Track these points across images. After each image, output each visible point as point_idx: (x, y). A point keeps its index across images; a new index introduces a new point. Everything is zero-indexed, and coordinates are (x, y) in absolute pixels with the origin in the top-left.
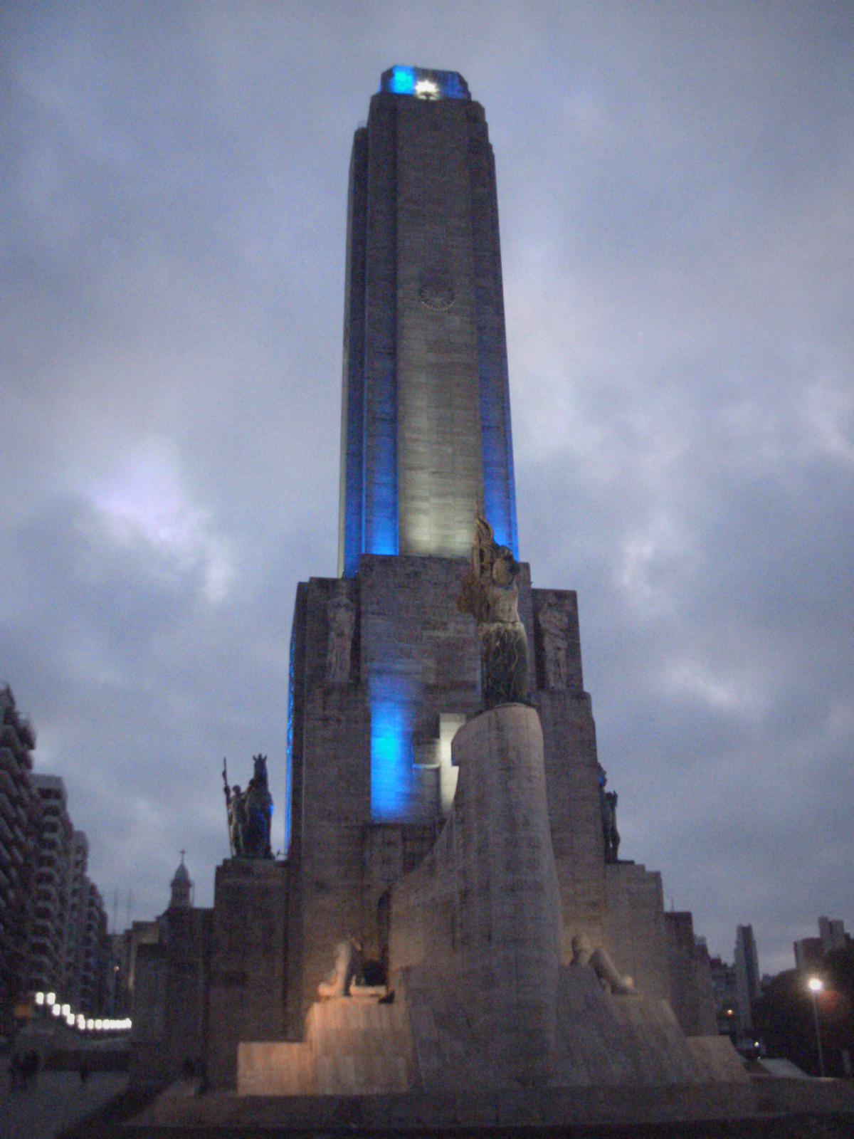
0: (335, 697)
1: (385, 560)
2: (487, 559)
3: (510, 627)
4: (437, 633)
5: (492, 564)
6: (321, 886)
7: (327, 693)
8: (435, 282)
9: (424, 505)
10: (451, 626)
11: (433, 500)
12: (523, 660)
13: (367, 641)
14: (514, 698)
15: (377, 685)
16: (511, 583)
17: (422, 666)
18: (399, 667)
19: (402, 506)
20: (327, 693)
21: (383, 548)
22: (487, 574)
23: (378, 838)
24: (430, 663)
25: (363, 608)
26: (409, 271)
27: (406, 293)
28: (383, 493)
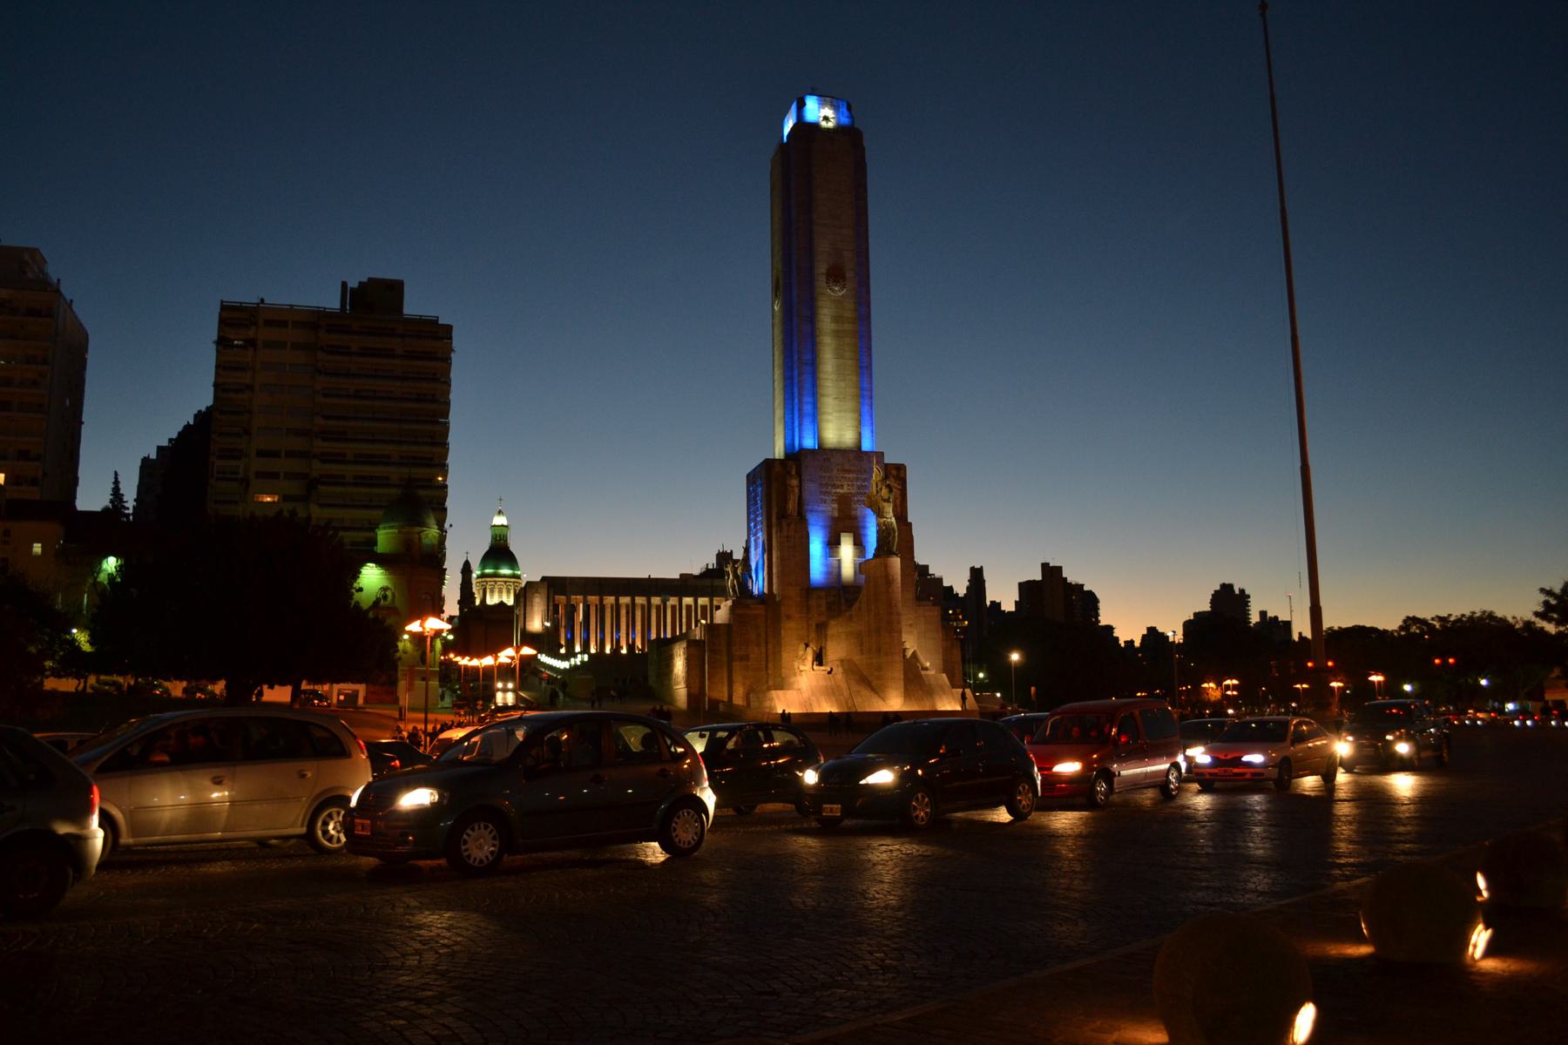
1: (812, 451)
6: (789, 617)
8: (836, 275)
13: (806, 495)
14: (891, 553)
15: (811, 518)
17: (831, 508)
21: (809, 443)
26: (821, 268)
27: (821, 282)
28: (808, 408)
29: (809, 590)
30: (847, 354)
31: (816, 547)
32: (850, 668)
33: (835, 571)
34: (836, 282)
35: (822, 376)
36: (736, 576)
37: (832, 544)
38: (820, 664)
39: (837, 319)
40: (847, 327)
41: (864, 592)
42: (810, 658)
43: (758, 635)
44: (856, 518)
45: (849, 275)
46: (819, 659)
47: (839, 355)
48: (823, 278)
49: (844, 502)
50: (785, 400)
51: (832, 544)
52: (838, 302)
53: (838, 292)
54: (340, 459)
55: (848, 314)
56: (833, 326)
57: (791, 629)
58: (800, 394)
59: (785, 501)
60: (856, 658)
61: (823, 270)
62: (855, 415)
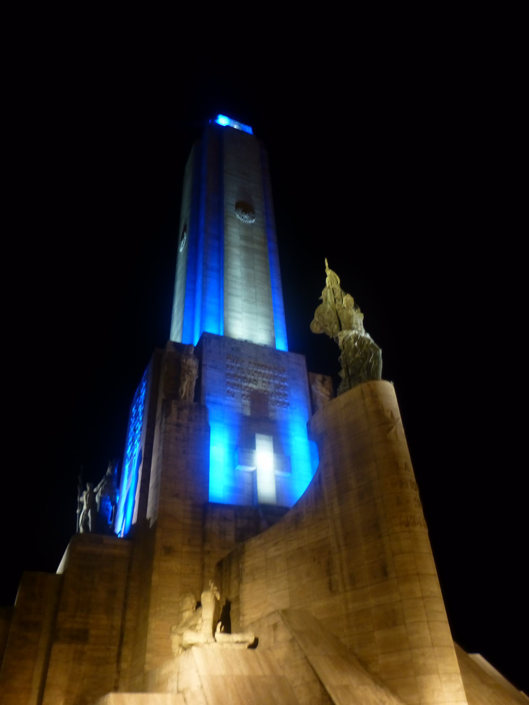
0: (186, 412)
4: (251, 385)
6: (169, 551)
7: (180, 409)
9: (239, 316)
10: (260, 383)
11: (244, 314)
13: (206, 383)
15: (214, 413)
18: (226, 402)
20: (180, 409)
24: (247, 402)
25: (204, 362)
26: (230, 201)
29: (205, 508)
31: (219, 446)
32: (306, 632)
33: (246, 487)
36: (92, 504)
37: (243, 446)
38: (227, 630)
41: (289, 515)
42: (208, 613)
44: (274, 422)
46: (225, 620)
47: (248, 264)
48: (234, 208)
49: (259, 400)
50: (183, 327)
51: (243, 446)
56: (243, 243)
57: (170, 570)
58: (204, 300)
59: (177, 384)
60: (318, 606)
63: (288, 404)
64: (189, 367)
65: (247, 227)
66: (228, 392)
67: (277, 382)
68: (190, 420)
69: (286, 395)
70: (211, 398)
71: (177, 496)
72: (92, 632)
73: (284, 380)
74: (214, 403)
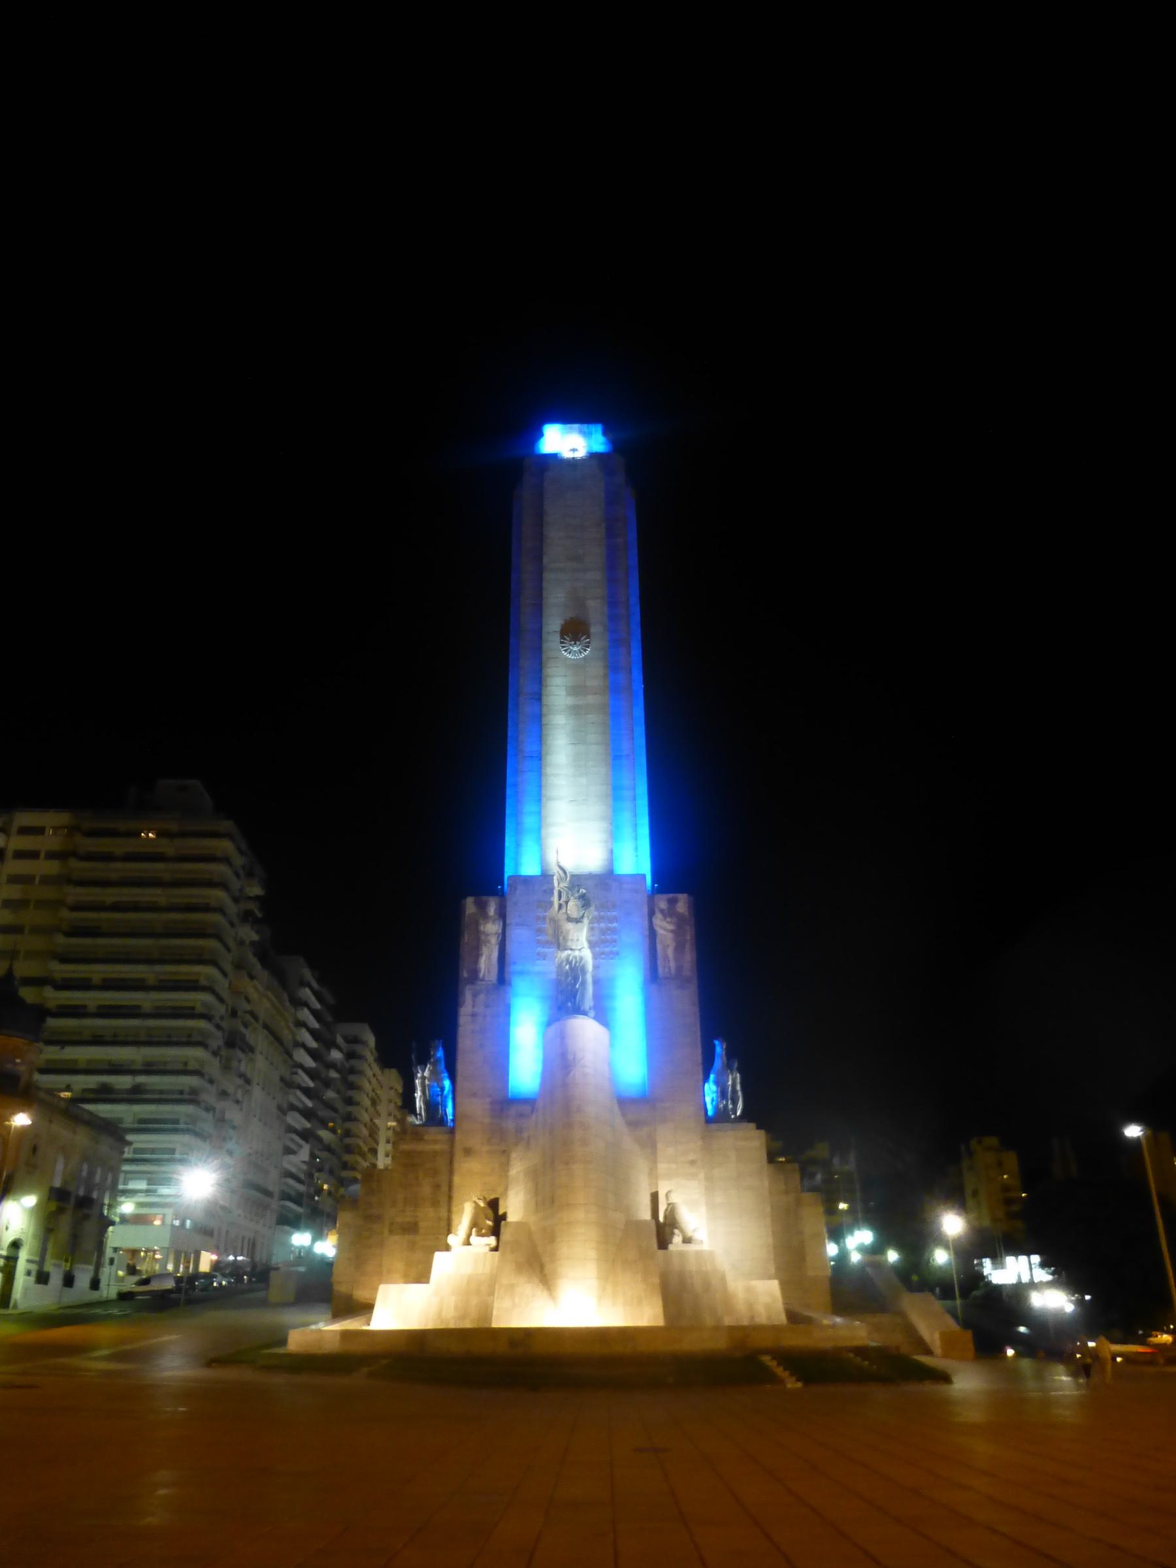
0: (482, 997)
2: (564, 899)
3: (577, 953)
5: (567, 903)
6: (468, 1152)
7: (475, 995)
8: (575, 631)
12: (584, 983)
13: (511, 948)
14: (578, 1011)
16: (583, 917)
19: (544, 831)
22: (563, 911)
23: (513, 1111)
25: (508, 922)
26: (553, 624)
30: (593, 737)
34: (576, 639)
35: (549, 770)
39: (576, 690)
40: (591, 699)
43: (437, 1187)
45: (595, 629)
47: (578, 739)
48: (557, 638)
52: (577, 667)
53: (573, 653)
54: (84, 985)
55: (593, 683)
56: (570, 701)
61: (558, 628)
62: (604, 825)
63: (617, 953)
64: (487, 935)
65: (577, 667)
66: (539, 954)
67: (602, 925)
68: (487, 1006)
69: (615, 941)
70: (517, 968)
71: (474, 1095)
72: (422, 1224)
73: (615, 919)
74: (521, 973)
